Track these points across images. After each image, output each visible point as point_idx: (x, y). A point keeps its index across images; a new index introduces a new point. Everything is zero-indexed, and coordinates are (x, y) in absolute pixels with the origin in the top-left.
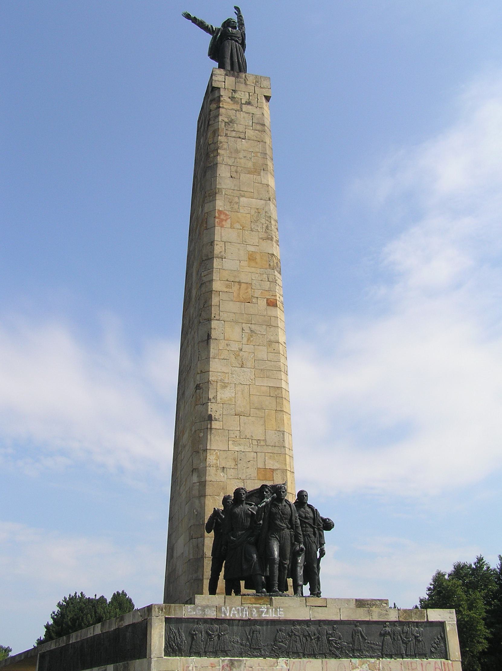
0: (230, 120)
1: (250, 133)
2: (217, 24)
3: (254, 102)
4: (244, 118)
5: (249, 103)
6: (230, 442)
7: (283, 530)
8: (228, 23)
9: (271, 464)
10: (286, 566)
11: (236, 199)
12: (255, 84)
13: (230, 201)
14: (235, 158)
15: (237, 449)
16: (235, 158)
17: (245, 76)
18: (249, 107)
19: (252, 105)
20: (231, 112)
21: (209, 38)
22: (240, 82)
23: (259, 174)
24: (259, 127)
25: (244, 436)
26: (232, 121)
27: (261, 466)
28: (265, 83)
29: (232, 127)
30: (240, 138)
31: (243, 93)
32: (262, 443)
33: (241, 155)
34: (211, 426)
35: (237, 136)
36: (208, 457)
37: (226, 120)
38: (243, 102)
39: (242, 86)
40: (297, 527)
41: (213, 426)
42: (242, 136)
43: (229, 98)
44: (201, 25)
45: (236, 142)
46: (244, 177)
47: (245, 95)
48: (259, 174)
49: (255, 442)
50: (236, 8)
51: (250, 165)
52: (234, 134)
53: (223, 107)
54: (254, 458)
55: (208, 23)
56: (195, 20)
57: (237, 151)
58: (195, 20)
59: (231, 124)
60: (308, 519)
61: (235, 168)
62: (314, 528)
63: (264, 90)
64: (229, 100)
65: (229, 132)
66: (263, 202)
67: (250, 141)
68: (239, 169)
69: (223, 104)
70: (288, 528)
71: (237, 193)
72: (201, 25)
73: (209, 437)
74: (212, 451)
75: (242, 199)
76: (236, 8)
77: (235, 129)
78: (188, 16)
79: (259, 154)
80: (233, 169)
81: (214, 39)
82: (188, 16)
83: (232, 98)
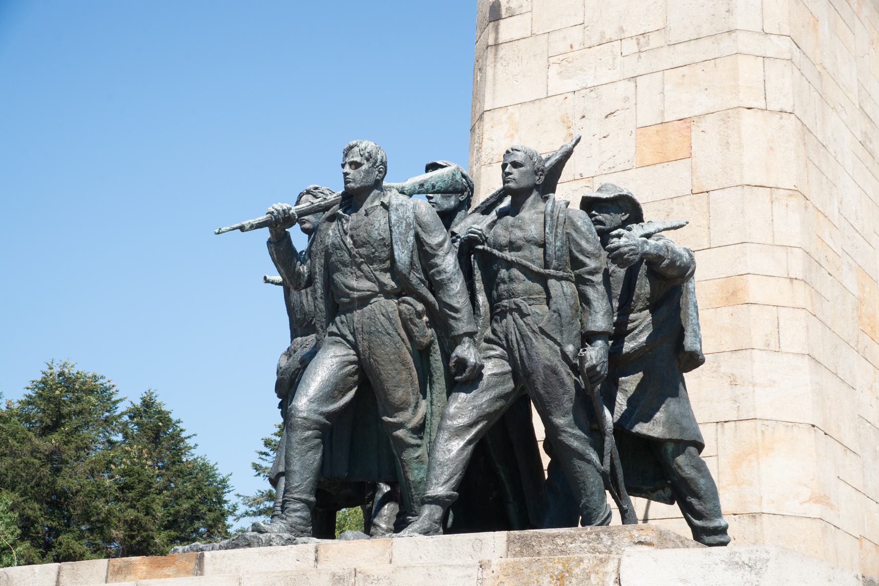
6: (554, 69)
7: (364, 301)
9: (683, 102)
10: (400, 433)
15: (572, 84)
25: (595, 39)
27: (648, 117)
32: (655, 41)
34: (496, 39)
36: (486, 136)
40: (436, 286)
41: (503, 36)
49: (630, 46)
54: (626, 99)
60: (519, 249)
62: (542, 279)
70: (388, 295)
73: (489, 71)
74: (498, 114)
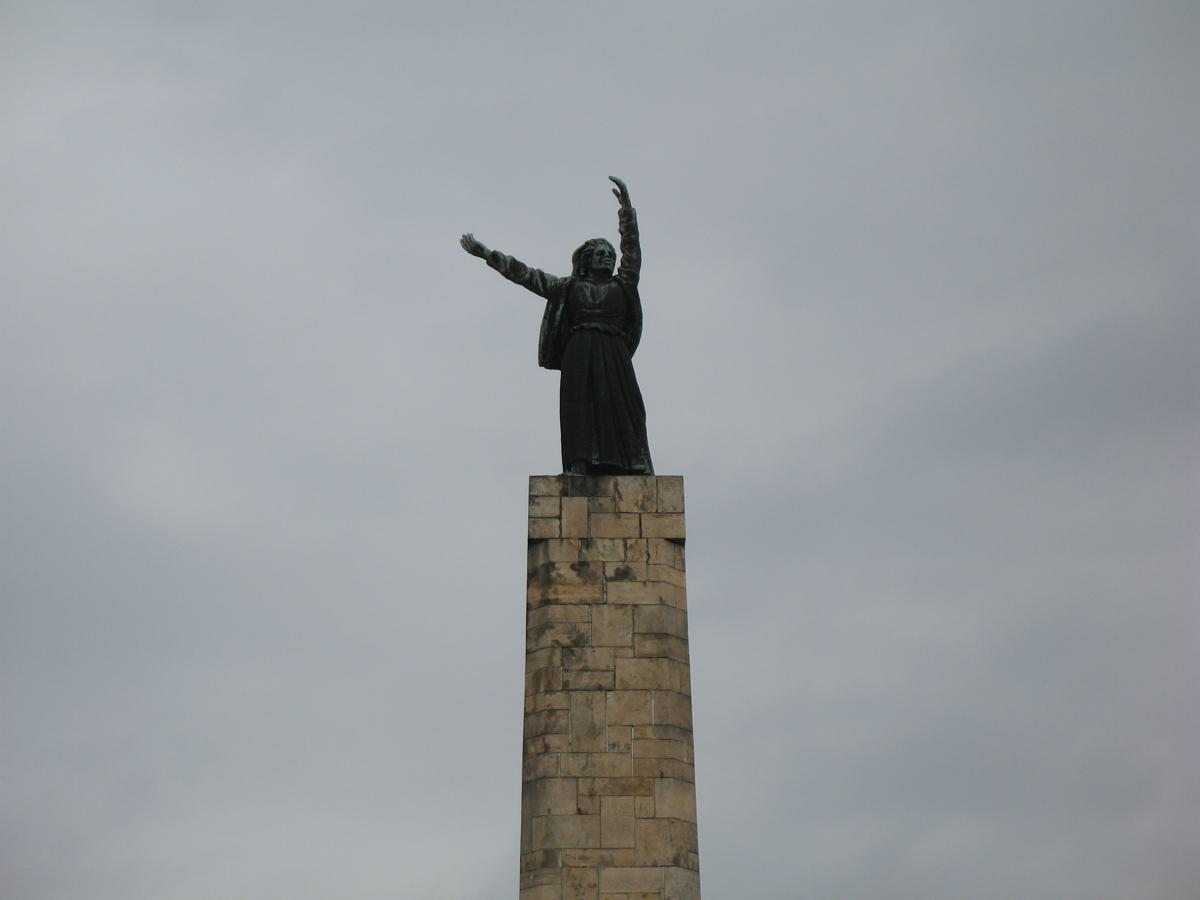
0: (574, 637)
1: (629, 669)
2: (561, 268)
3: (639, 568)
4: (611, 624)
5: (623, 574)
8: (589, 257)
11: (591, 876)
12: (643, 507)
13: (577, 882)
14: (589, 753)
16: (589, 753)
17: (616, 485)
18: (626, 585)
19: (633, 579)
20: (575, 611)
21: (536, 306)
22: (601, 510)
23: (650, 792)
24: (650, 646)
26: (579, 642)
28: (668, 497)
29: (580, 659)
30: (600, 688)
31: (608, 543)
33: (603, 742)
35: (595, 682)
37: (565, 640)
38: (610, 572)
39: (607, 521)
42: (606, 682)
43: (573, 567)
44: (514, 271)
45: (589, 704)
46: (613, 807)
47: (614, 548)
48: (650, 792)
50: (613, 179)
51: (625, 767)
52: (585, 680)
53: (556, 602)
55: (532, 262)
56: (495, 260)
57: (594, 732)
58: (495, 260)
59: (577, 651)
61: (589, 781)
63: (666, 521)
64: (571, 575)
65: (571, 677)
66: (659, 872)
67: (627, 695)
68: (599, 784)
69: (556, 592)
71: (595, 855)
72: (514, 271)
75: (606, 873)
76: (613, 179)
77: (590, 665)
78: (475, 249)
79: (649, 732)
80: (584, 788)
81: (549, 316)
82: (475, 249)
83: (580, 567)
